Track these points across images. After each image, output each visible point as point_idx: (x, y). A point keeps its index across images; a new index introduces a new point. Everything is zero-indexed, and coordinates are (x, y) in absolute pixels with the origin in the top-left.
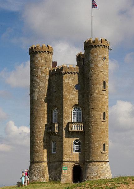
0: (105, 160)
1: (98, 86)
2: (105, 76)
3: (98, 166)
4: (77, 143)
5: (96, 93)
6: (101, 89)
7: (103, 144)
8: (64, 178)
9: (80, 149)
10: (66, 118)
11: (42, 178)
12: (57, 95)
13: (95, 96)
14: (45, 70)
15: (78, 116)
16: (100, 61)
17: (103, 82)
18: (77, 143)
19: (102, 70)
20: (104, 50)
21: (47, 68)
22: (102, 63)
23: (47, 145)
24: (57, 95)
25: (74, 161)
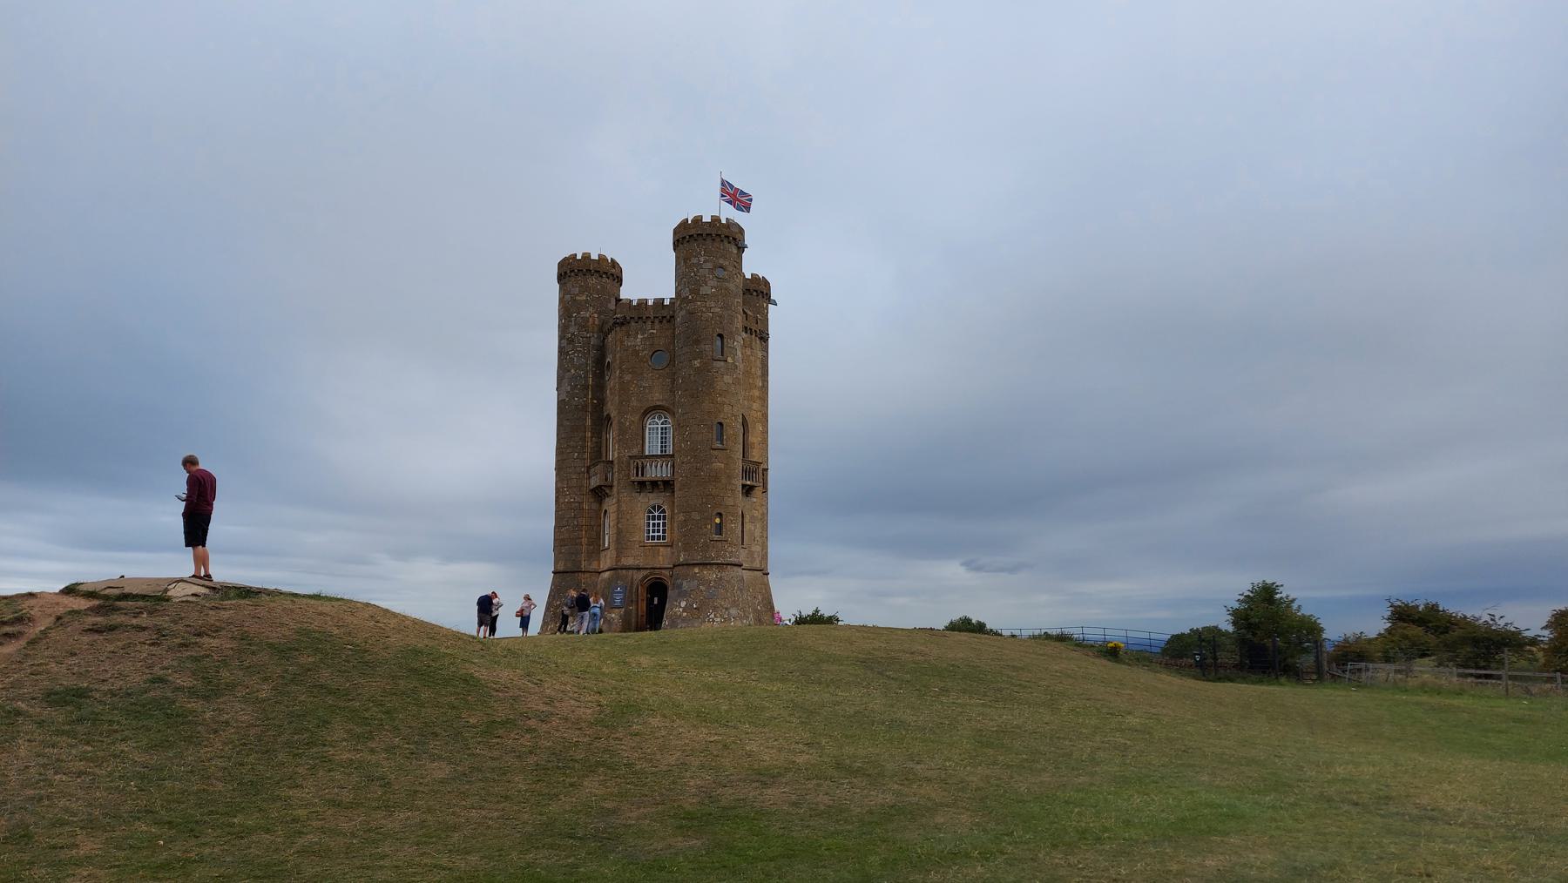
4: (656, 514)
9: (664, 531)
14: (586, 320)
18: (656, 514)
21: (596, 315)
22: (711, 283)
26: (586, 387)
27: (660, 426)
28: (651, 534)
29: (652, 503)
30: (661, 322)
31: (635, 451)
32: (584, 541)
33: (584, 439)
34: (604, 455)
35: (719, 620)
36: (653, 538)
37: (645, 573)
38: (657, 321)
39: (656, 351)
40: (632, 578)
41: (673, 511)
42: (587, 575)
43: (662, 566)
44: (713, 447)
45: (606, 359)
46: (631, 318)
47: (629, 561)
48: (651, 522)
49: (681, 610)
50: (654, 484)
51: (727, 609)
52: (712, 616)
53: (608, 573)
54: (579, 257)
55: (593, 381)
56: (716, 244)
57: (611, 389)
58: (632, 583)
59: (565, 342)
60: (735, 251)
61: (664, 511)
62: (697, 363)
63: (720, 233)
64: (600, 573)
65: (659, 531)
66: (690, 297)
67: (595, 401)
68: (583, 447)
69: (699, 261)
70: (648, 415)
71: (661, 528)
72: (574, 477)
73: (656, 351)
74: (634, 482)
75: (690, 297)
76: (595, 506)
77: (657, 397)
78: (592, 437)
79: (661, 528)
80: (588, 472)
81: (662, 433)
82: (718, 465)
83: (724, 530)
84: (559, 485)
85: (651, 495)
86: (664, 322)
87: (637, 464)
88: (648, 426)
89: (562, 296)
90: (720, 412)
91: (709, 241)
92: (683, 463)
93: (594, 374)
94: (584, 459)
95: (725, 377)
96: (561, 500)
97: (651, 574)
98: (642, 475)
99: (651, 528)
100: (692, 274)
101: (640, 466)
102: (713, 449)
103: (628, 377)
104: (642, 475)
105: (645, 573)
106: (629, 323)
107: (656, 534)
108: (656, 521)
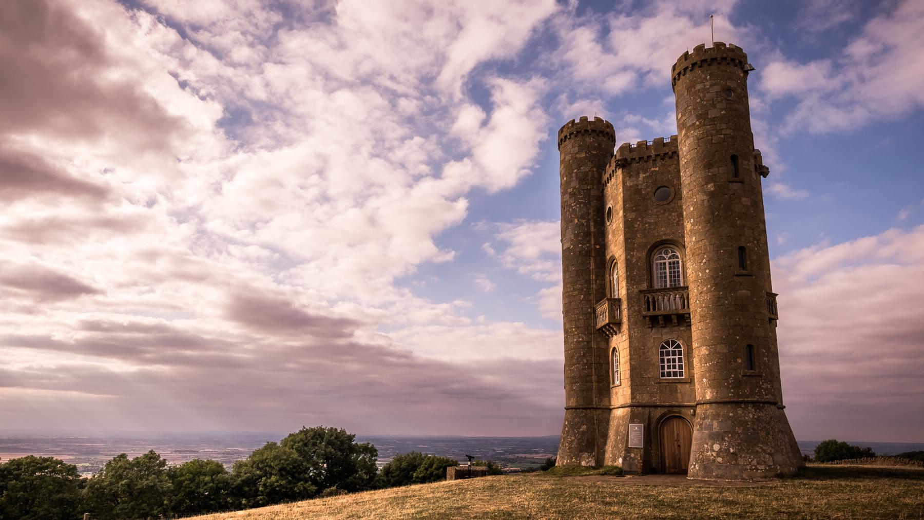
0: (756, 398)
3: (733, 417)
4: (671, 349)
9: (681, 367)
11: (586, 455)
12: (614, 226)
15: (670, 273)
21: (595, 169)
22: (719, 106)
23: (601, 361)
25: (664, 404)
26: (588, 234)
27: (667, 261)
28: (666, 370)
29: (665, 338)
31: (644, 286)
32: (594, 378)
34: (616, 288)
35: (762, 467)
36: (669, 374)
37: (666, 410)
38: (659, 159)
39: (659, 188)
42: (599, 412)
43: (681, 404)
45: (606, 205)
47: (646, 399)
48: (666, 358)
49: (714, 454)
51: (769, 454)
52: (755, 462)
53: (622, 409)
54: (577, 121)
55: (595, 228)
57: (613, 232)
59: (567, 197)
60: (742, 75)
61: (679, 346)
64: (611, 410)
65: (674, 367)
66: (698, 123)
67: (598, 247)
68: (589, 289)
70: (655, 251)
71: (677, 364)
72: (581, 317)
73: (659, 188)
74: (644, 317)
76: (603, 345)
78: (596, 280)
79: (677, 364)
81: (670, 268)
84: (568, 326)
85: (665, 330)
87: (648, 298)
88: (655, 262)
90: (741, 236)
93: (596, 222)
94: (590, 300)
95: (744, 199)
96: (570, 341)
97: (669, 412)
98: (654, 309)
99: (666, 364)
101: (650, 300)
102: (737, 275)
104: (654, 309)
106: (630, 164)
107: (672, 370)
108: (671, 357)
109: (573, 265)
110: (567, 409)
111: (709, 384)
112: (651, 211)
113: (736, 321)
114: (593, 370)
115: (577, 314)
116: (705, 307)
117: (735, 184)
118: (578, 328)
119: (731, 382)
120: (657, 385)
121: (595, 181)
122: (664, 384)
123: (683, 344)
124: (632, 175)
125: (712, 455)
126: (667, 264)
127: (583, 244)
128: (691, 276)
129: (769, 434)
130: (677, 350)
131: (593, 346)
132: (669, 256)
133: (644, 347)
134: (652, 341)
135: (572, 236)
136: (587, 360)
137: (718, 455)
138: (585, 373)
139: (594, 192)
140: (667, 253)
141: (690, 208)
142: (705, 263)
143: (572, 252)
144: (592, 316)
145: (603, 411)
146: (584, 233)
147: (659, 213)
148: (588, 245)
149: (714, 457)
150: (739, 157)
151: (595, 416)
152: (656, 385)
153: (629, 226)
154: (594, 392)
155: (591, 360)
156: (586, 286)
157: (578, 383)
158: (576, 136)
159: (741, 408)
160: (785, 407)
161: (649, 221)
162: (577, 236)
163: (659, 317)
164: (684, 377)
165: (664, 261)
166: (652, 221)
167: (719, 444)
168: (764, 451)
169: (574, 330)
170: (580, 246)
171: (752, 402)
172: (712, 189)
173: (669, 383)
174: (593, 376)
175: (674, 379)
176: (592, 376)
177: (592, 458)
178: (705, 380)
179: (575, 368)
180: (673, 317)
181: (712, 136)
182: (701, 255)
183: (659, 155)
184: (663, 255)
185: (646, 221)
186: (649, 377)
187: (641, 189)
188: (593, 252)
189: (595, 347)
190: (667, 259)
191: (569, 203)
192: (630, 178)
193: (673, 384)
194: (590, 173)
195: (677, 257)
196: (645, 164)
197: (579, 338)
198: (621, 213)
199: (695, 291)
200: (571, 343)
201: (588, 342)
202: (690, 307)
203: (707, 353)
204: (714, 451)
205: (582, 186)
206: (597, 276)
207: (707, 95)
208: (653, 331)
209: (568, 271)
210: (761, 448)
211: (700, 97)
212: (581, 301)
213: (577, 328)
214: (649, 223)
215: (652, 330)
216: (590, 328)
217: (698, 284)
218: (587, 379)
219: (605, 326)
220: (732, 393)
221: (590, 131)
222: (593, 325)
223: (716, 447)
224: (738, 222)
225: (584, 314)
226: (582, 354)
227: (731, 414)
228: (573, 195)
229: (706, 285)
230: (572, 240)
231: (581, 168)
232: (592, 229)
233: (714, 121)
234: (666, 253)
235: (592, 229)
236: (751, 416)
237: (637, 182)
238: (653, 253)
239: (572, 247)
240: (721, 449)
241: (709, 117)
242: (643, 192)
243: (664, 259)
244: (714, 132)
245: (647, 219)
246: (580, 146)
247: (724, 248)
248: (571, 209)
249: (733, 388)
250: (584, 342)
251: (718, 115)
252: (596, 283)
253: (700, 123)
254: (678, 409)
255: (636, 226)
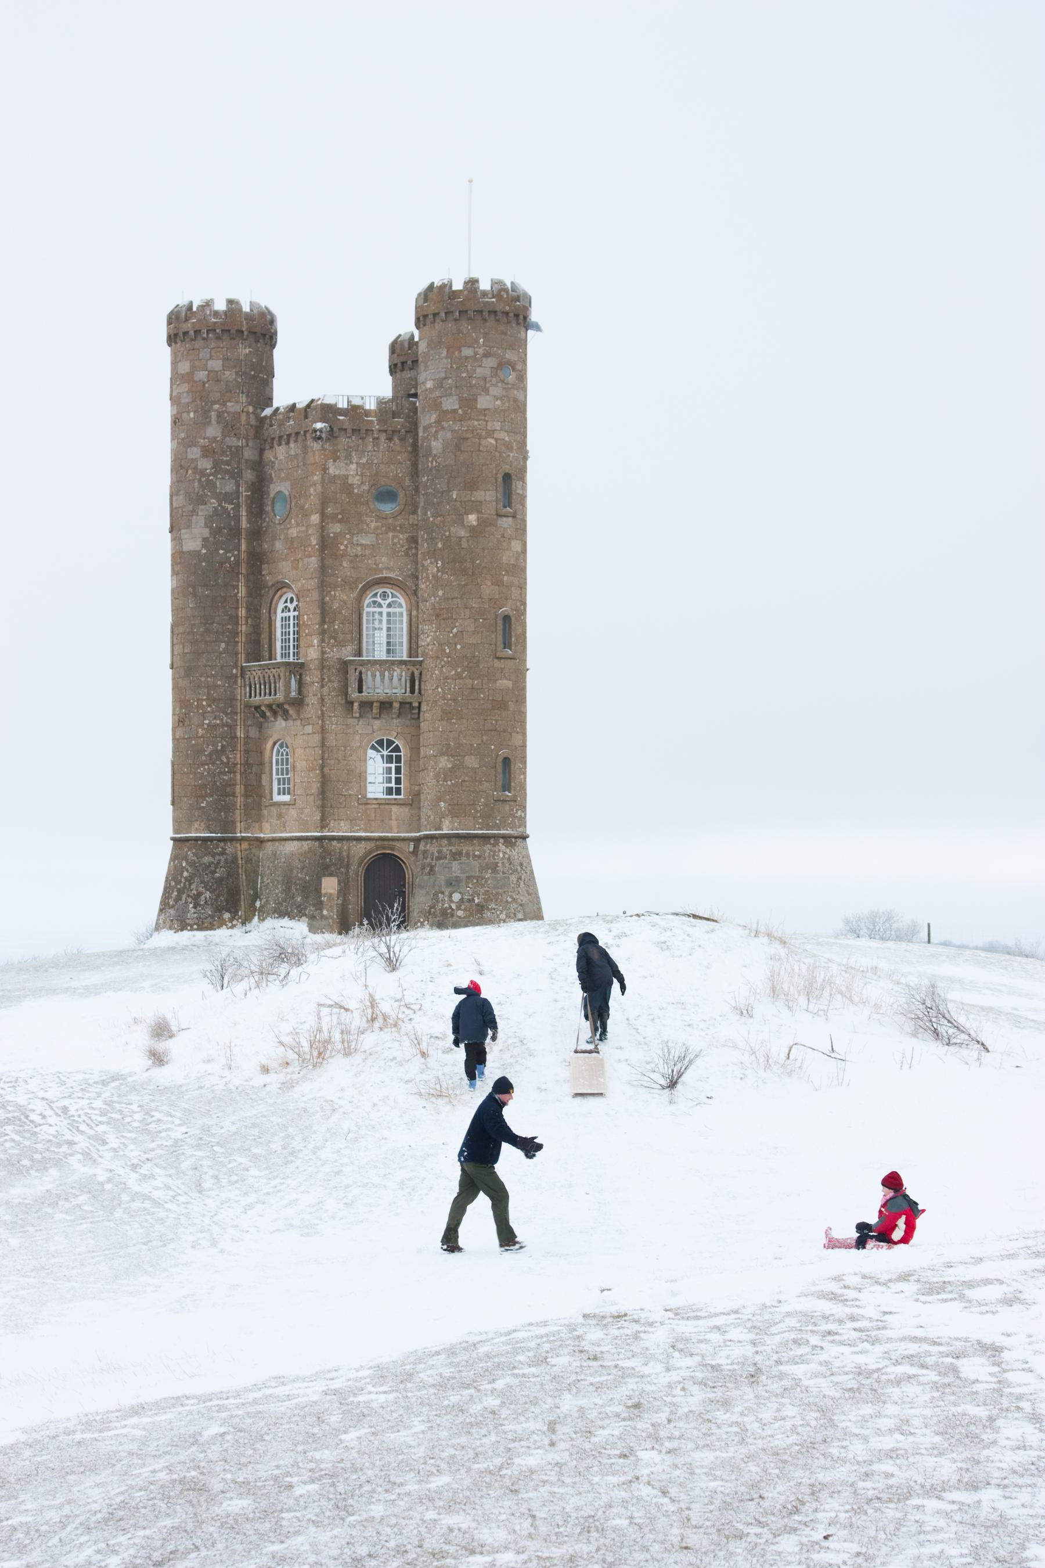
1: (479, 495)
2: (510, 449)
3: (479, 857)
4: (385, 753)
5: (472, 529)
6: (489, 510)
7: (500, 759)
8: (325, 912)
9: (398, 781)
10: (335, 639)
12: (293, 532)
13: (464, 544)
16: (488, 385)
17: (500, 479)
19: (497, 425)
20: (506, 334)
21: (251, 409)
22: (495, 391)
23: (251, 761)
24: (293, 532)
30: (390, 439)
32: (239, 789)
33: (235, 619)
37: (371, 845)
38: (383, 437)
40: (348, 856)
41: (415, 750)
44: (499, 654)
46: (341, 429)
50: (385, 706)
51: (521, 905)
53: (296, 843)
55: (249, 521)
56: (502, 328)
58: (348, 856)
59: (194, 453)
61: (397, 749)
62: (472, 519)
63: (507, 308)
68: (236, 633)
69: (476, 353)
70: (368, 592)
72: (219, 683)
75: (460, 411)
76: (253, 733)
77: (388, 565)
78: (247, 618)
79: (393, 776)
80: (242, 676)
81: (389, 622)
82: (505, 683)
83: (512, 784)
85: (377, 724)
86: (396, 440)
87: (361, 673)
88: (366, 610)
89: (185, 367)
90: (507, 599)
91: (492, 322)
92: (447, 678)
93: (249, 510)
97: (377, 848)
100: (464, 375)
103: (335, 528)
105: (371, 845)
109: (206, 585)
110: (172, 839)
111: (449, 811)
112: (368, 525)
113: (492, 723)
114: (238, 776)
115: (212, 676)
116: (451, 700)
117: (505, 519)
118: (214, 700)
119: (479, 809)
120: (363, 807)
121: (252, 433)
122: (374, 806)
123: (405, 747)
124: (339, 458)
125: (450, 907)
126: (385, 615)
127: (227, 551)
128: (430, 648)
129: (520, 878)
130: (394, 754)
131: (238, 734)
132: (387, 602)
133: (345, 747)
134: (357, 738)
135: (206, 533)
136: (228, 758)
137: (459, 908)
138: (224, 780)
139: (249, 454)
140: (384, 596)
141: (437, 544)
142: (456, 634)
143: (204, 561)
144: (239, 681)
145: (249, 845)
146: (231, 529)
147: (379, 531)
148: (236, 553)
149: (453, 910)
150: (513, 477)
151: (239, 852)
152: (360, 807)
153: (326, 545)
154: (238, 812)
155: (235, 758)
156: (230, 627)
157: (212, 796)
158: (218, 338)
159: (491, 844)
160: (528, 837)
161: (364, 542)
162: (214, 532)
163: (375, 704)
164: (401, 797)
165: (380, 610)
166: (368, 543)
167: (460, 893)
168: (514, 900)
169: (204, 703)
170: (221, 552)
171: (504, 837)
172: (475, 523)
173: (379, 804)
174: (238, 786)
175: (389, 799)
176: (235, 785)
177: (237, 920)
178: (442, 804)
179: (205, 769)
180: (396, 705)
181: (479, 439)
182: (450, 621)
183: (385, 431)
184: (379, 600)
185: (357, 540)
186: (350, 795)
187: (352, 485)
188: (244, 565)
189: (242, 736)
190: (385, 606)
191: (199, 467)
192: (335, 461)
193: (387, 806)
194: (244, 417)
195: (400, 606)
196: (360, 441)
197: (215, 718)
198: (315, 518)
199: (437, 672)
200: (198, 726)
201: (230, 726)
202: (423, 692)
203: (449, 766)
204: (453, 902)
205: (228, 438)
206: (248, 610)
207: (479, 370)
208: (360, 723)
209: (194, 595)
210: (511, 897)
211: (468, 371)
212: (221, 653)
213: (211, 700)
214: (362, 545)
215: (359, 721)
216: (234, 702)
217: (443, 663)
218: (228, 789)
219: (270, 706)
220: (479, 823)
221: (245, 333)
222: (239, 698)
223: (456, 897)
224: (505, 578)
225: (227, 677)
226: (219, 748)
227: (477, 853)
228: (206, 452)
229: (455, 668)
230: (205, 540)
231: (229, 404)
232: (244, 524)
233: (485, 415)
234: (384, 596)
235: (244, 524)
236: (501, 855)
237: (347, 470)
238: (364, 597)
239: (204, 551)
240: (462, 899)
241: (478, 407)
242: (356, 491)
243: (380, 606)
244: (484, 433)
245: (359, 538)
246: (226, 359)
247: (485, 617)
248: (203, 479)
249: (481, 817)
250: (223, 725)
251: (491, 406)
252: (246, 624)
253: (465, 413)
254: (391, 843)
255: (342, 547)
